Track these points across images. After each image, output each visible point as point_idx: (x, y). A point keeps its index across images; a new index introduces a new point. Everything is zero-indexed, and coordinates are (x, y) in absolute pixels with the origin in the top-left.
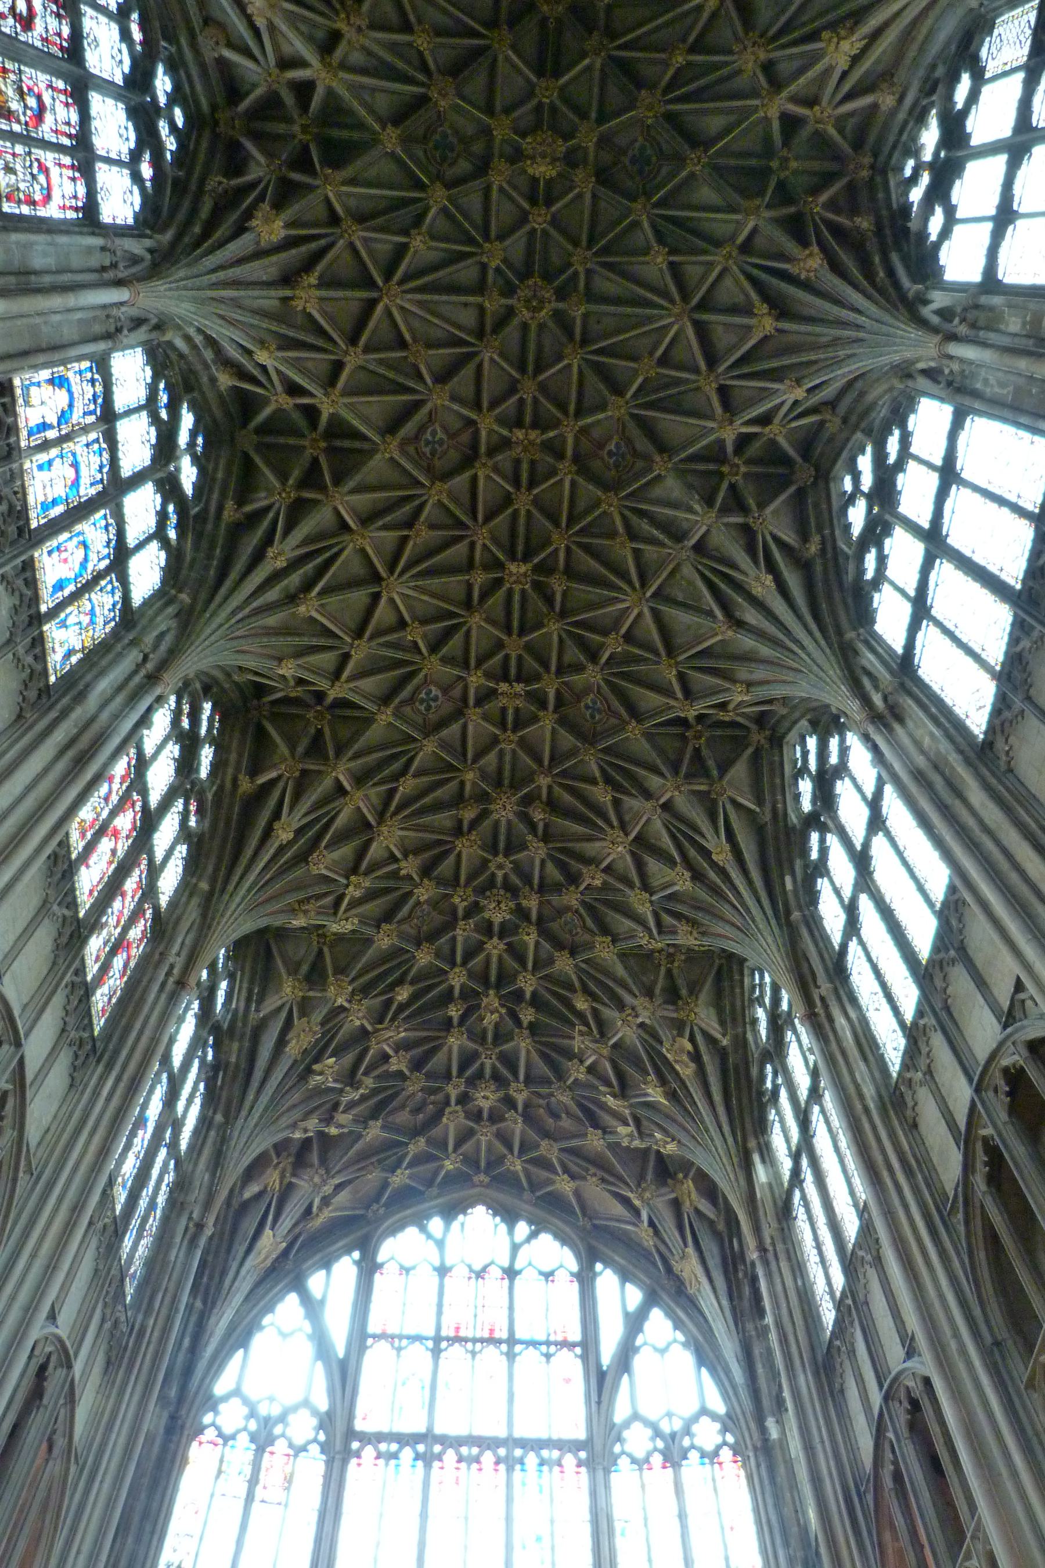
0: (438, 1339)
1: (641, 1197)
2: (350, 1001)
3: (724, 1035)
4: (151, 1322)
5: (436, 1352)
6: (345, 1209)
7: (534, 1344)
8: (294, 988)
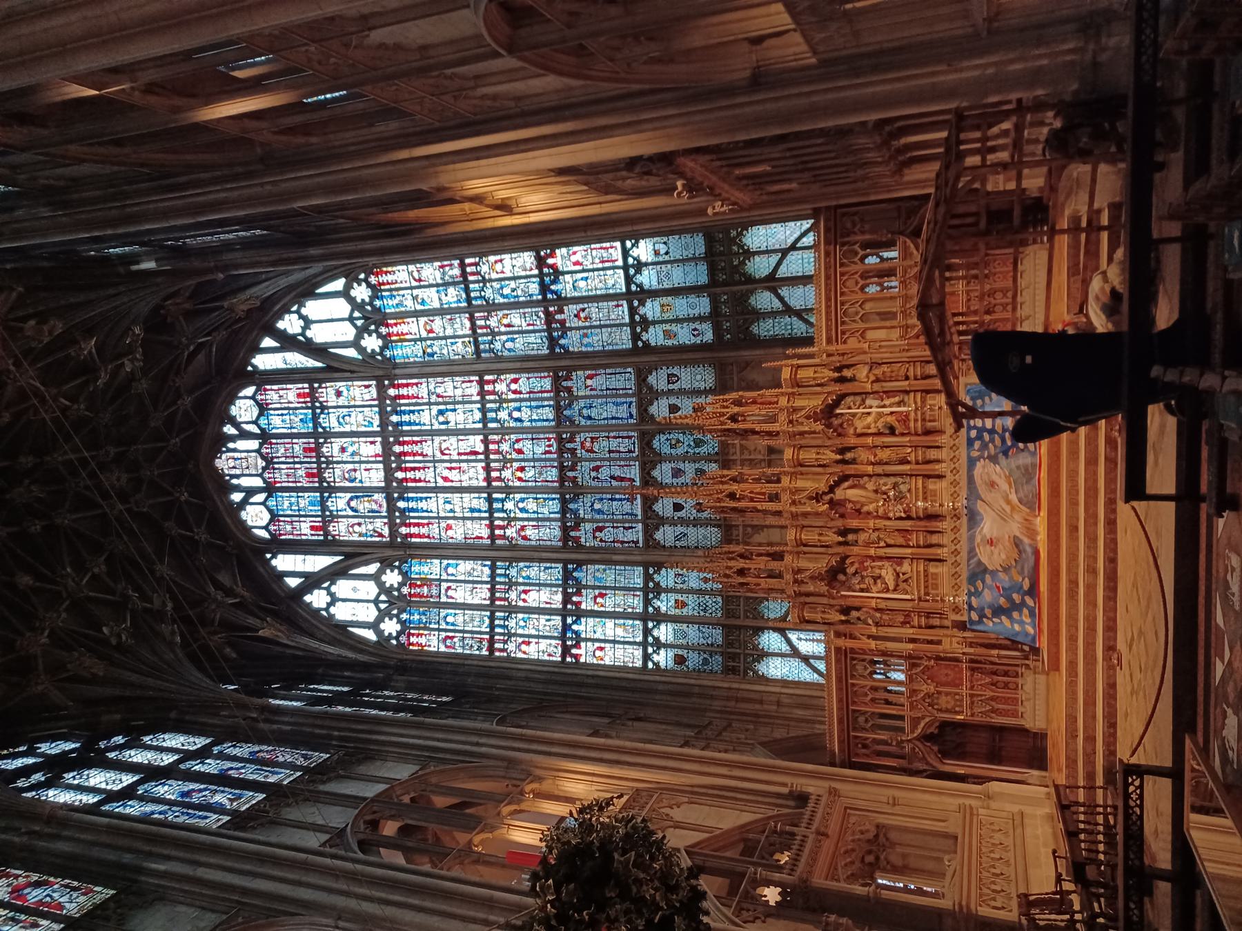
0: (320, 490)
1: (188, 346)
2: (43, 630)
3: (13, 289)
4: (336, 733)
5: (333, 490)
6: (234, 576)
7: (315, 418)
8: (37, 684)
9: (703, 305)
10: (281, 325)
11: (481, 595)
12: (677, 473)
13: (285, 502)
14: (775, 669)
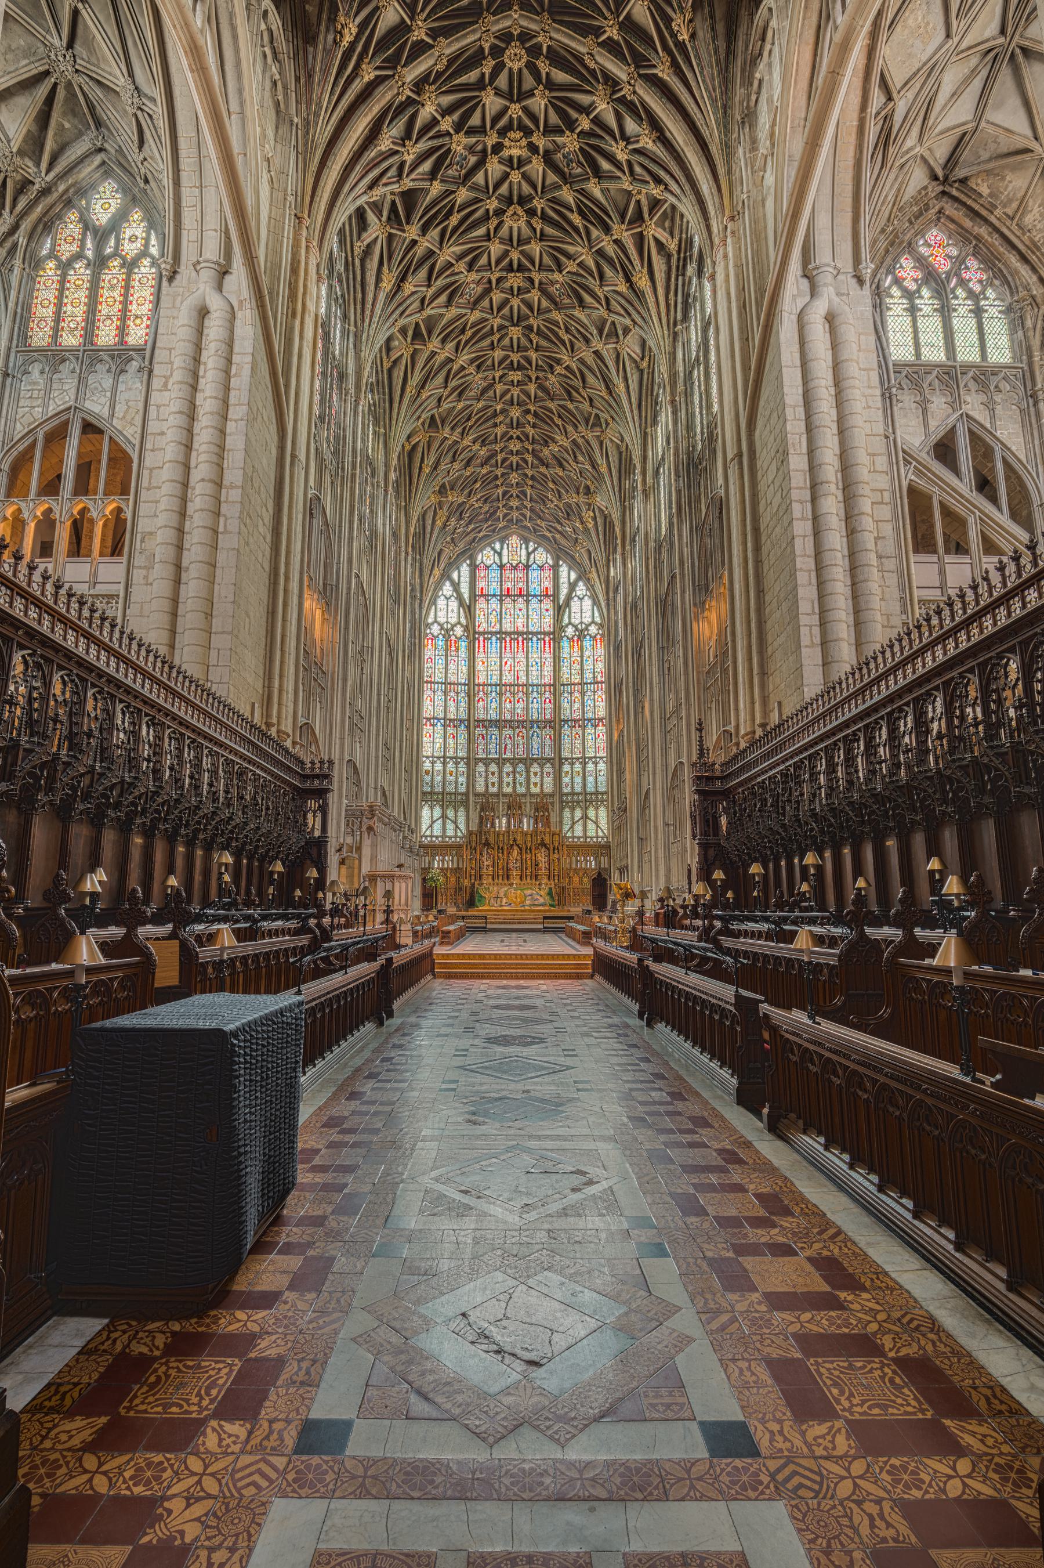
0: (501, 595)
5: (501, 601)
7: (535, 596)
9: (578, 789)
10: (581, 584)
11: (452, 678)
12: (508, 774)
13: (494, 574)
14: (426, 812)
